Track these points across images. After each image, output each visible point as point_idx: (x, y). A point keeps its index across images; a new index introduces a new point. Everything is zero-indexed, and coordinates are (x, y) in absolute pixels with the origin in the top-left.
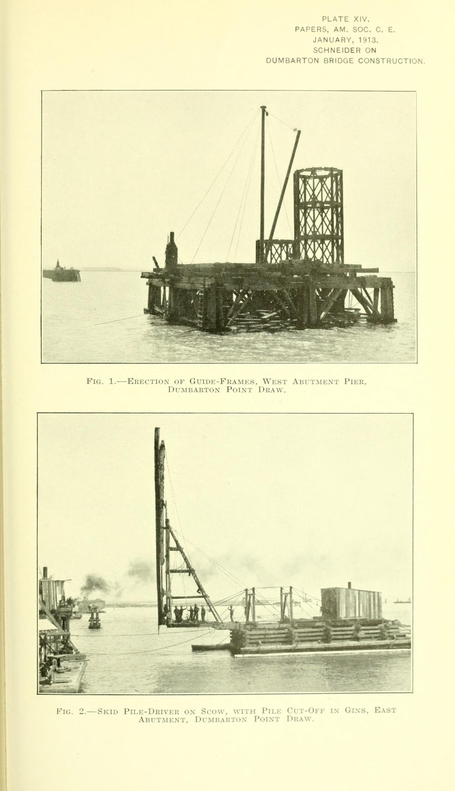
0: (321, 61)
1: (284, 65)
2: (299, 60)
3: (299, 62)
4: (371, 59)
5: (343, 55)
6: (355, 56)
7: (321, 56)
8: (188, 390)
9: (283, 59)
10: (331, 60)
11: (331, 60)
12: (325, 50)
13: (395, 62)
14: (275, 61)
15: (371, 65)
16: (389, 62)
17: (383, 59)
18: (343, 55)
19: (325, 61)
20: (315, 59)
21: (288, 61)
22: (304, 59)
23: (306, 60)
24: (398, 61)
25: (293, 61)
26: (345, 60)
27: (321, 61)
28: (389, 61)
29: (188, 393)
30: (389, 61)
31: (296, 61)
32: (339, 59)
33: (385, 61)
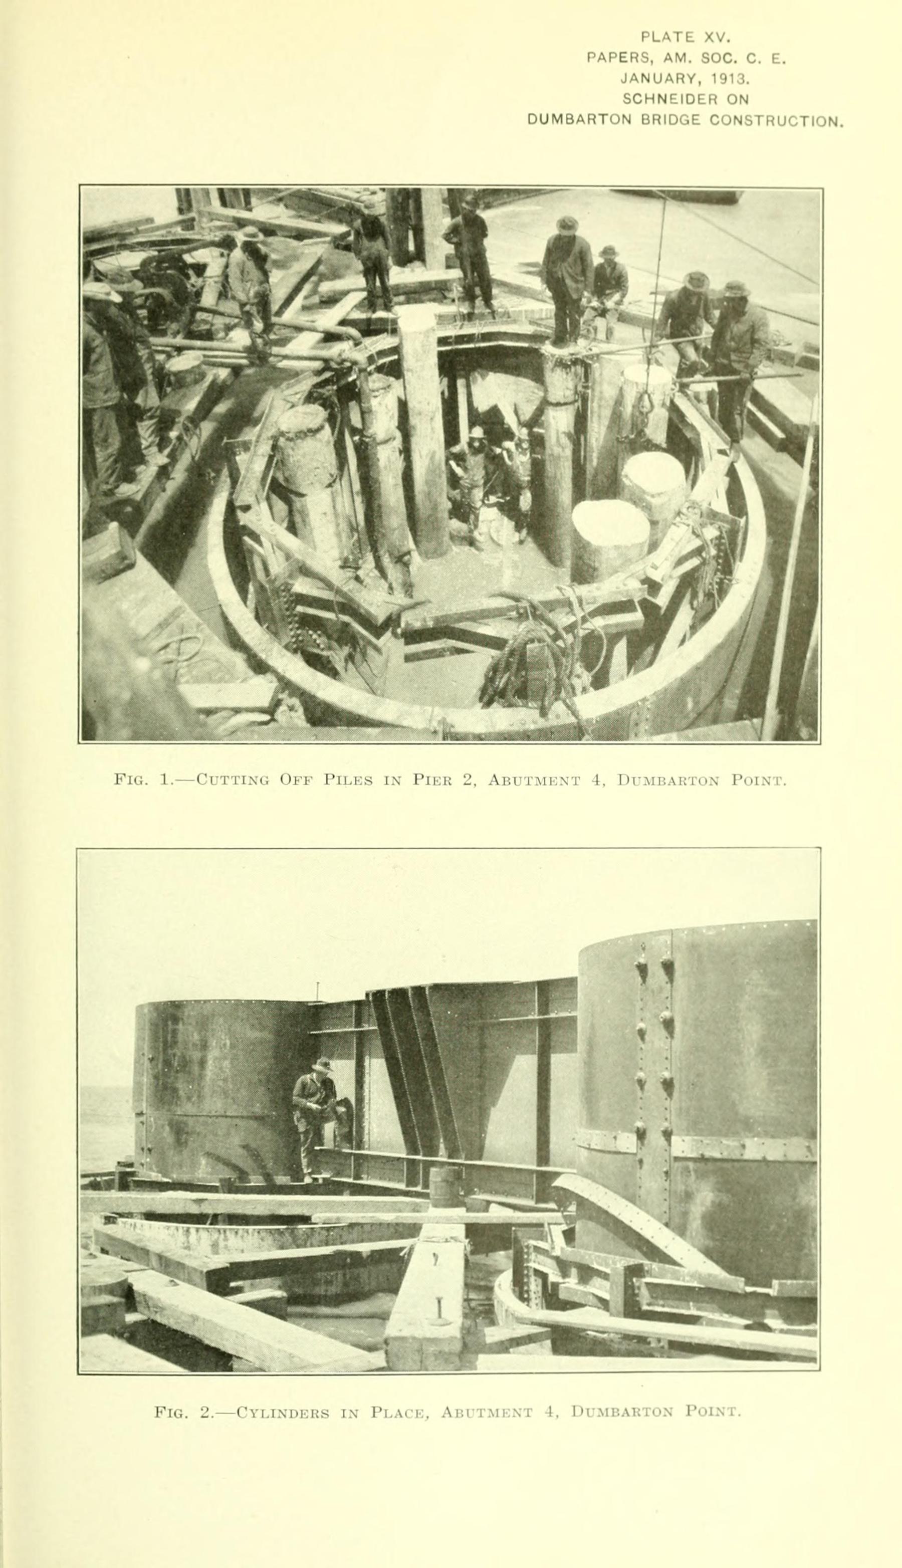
0: (636, 120)
1: (563, 127)
2: (592, 118)
3: (591, 122)
4: (735, 117)
5: (681, 109)
6: (704, 111)
7: (635, 111)
8: (656, 781)
9: (561, 116)
10: (657, 119)
11: (657, 119)
12: (646, 98)
13: (782, 122)
14: (544, 120)
15: (735, 128)
16: (770, 123)
17: (759, 117)
18: (681, 109)
19: (645, 120)
20: (624, 116)
21: (570, 120)
22: (603, 115)
23: (607, 118)
24: (787, 121)
25: (581, 119)
26: (684, 118)
27: (636, 120)
28: (770, 120)
29: (656, 787)
30: (770, 120)
31: (586, 120)
32: (670, 115)
33: (763, 120)
